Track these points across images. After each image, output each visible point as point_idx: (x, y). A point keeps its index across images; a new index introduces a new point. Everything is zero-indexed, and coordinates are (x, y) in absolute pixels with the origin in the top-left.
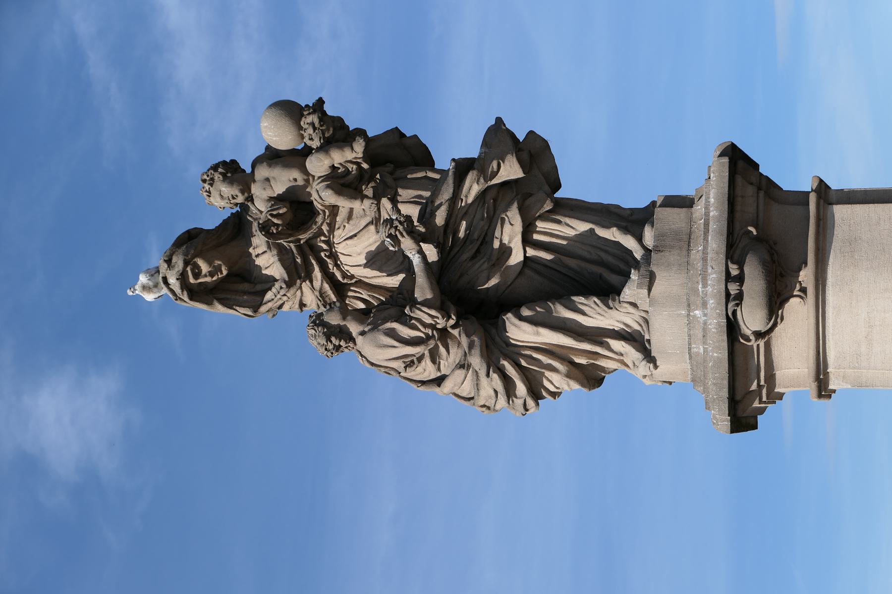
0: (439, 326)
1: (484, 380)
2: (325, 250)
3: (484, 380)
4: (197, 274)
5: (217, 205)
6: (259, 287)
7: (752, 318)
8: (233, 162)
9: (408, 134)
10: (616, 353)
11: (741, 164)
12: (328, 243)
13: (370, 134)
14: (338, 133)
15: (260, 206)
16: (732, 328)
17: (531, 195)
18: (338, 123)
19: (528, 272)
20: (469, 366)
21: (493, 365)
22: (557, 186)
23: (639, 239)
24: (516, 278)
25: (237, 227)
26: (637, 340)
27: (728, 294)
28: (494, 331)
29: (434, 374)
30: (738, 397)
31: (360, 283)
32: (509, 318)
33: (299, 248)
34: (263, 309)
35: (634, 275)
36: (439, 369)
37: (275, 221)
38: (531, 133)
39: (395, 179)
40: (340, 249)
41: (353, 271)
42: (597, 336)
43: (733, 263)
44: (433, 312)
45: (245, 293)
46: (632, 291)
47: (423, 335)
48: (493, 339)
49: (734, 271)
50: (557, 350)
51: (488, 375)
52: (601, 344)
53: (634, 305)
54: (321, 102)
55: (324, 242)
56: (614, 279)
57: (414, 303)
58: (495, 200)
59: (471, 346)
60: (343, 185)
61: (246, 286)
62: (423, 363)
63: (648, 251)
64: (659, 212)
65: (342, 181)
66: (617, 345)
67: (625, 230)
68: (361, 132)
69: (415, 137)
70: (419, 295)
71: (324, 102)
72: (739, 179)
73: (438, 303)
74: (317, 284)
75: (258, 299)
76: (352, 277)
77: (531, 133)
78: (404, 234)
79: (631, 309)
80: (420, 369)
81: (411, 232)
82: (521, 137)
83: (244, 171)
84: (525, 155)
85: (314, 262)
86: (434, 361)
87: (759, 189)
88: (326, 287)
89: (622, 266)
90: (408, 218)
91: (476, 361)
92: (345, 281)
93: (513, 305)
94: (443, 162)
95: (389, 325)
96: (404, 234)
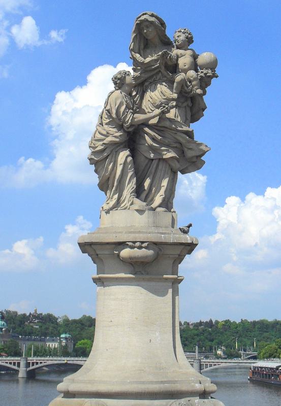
1: (101, 143)
2: (156, 78)
3: (101, 143)
4: (147, 27)
5: (174, 33)
6: (142, 52)
7: (125, 253)
8: (193, 41)
10: (112, 196)
11: (189, 248)
12: (160, 79)
13: (204, 97)
14: (204, 82)
15: (175, 52)
16: (122, 245)
17: (179, 162)
18: (208, 84)
19: (147, 161)
20: (107, 136)
21: (107, 146)
22: (183, 172)
23: (160, 206)
24: (145, 156)
25: (167, 43)
26: (117, 205)
27: (134, 242)
28: (122, 146)
29: (104, 122)
30: (92, 246)
32: (127, 152)
33: (158, 67)
34: (133, 53)
35: (145, 204)
38: (204, 162)
39: (185, 107)
42: (120, 190)
43: (148, 244)
44: (130, 121)
45: (139, 46)
46: (139, 204)
48: (119, 146)
49: (144, 245)
50: (113, 172)
51: (104, 144)
52: (116, 190)
53: (132, 204)
54: (217, 77)
55: (160, 78)
56: (143, 195)
57: (133, 113)
58: (176, 147)
59: (115, 137)
60: (182, 86)
61: (142, 47)
63: (154, 210)
64: (169, 214)
65: (184, 85)
66: (116, 196)
67: (164, 200)
68: (205, 93)
70: (136, 115)
72: (183, 247)
73: (133, 124)
74: (143, 75)
75: (137, 51)
77: (204, 162)
79: (130, 203)
81: (163, 113)
82: (202, 158)
83: (189, 46)
84: (195, 160)
85: (152, 74)
87: (179, 255)
88: (142, 79)
89: (150, 199)
90: (168, 112)
91: (110, 139)
93: (133, 154)
94: (193, 127)
95: (125, 103)
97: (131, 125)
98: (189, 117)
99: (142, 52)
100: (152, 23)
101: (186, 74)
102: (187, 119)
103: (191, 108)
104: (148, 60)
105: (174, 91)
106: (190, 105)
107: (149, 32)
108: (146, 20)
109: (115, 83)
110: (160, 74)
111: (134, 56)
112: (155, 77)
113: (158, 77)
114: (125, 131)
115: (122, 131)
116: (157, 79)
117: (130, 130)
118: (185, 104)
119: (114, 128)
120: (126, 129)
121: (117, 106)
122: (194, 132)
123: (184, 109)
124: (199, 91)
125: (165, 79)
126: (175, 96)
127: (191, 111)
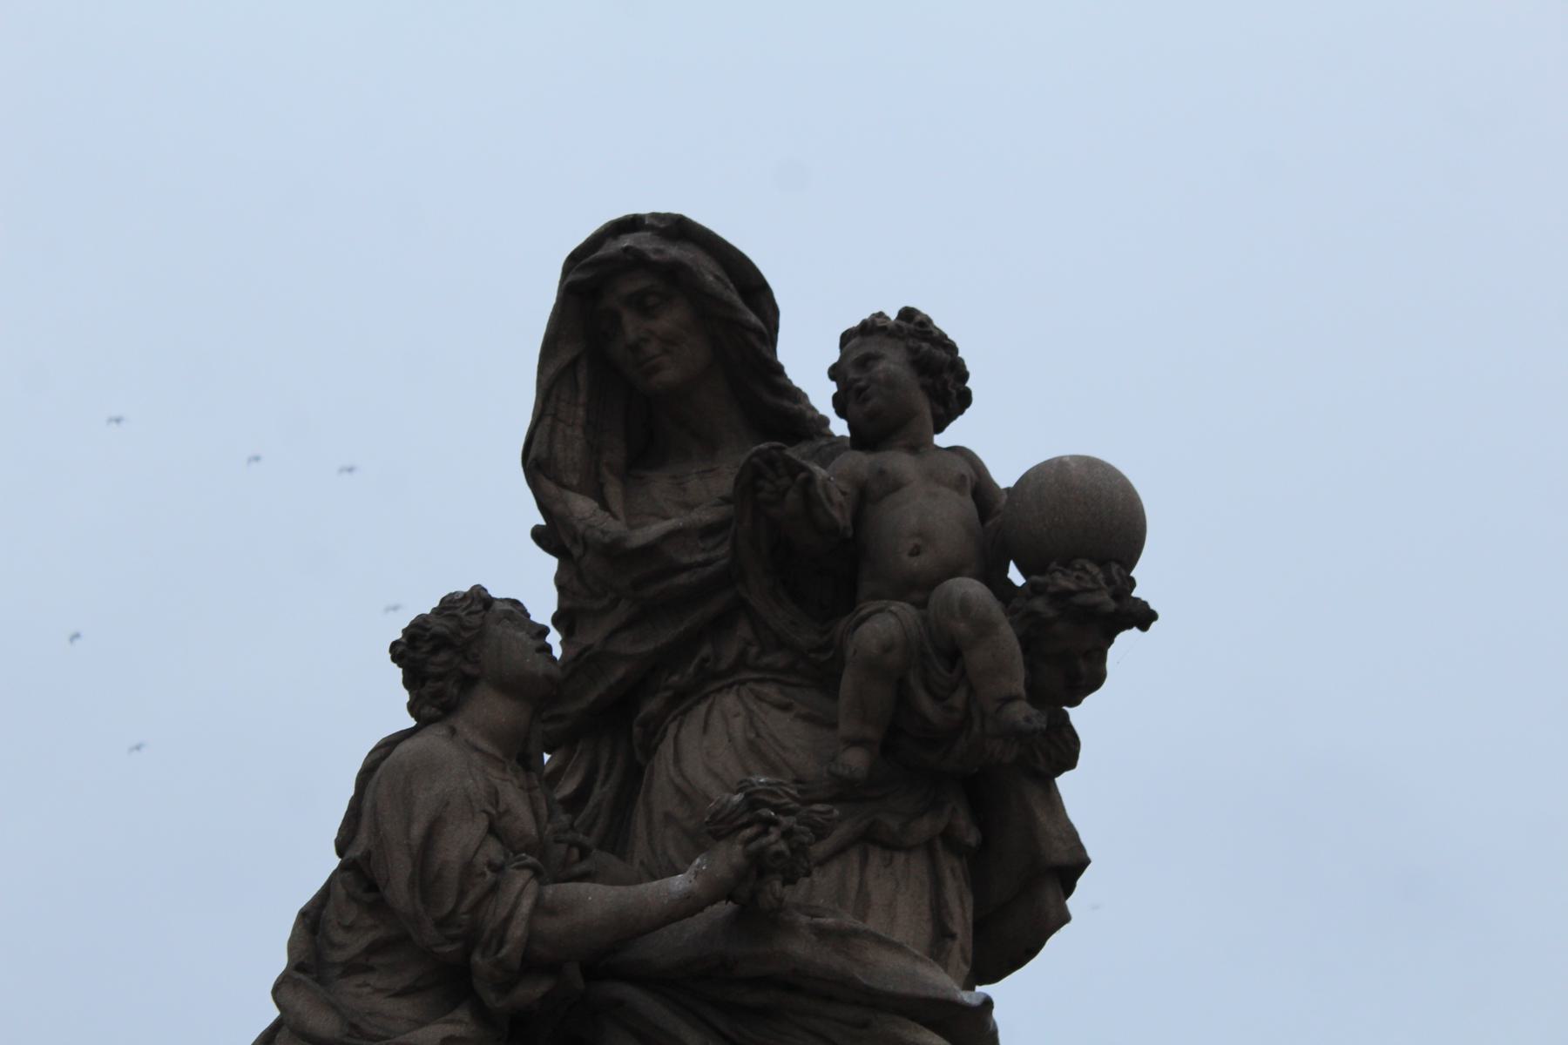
0: (477, 958)
4: (640, 304)
6: (614, 491)
8: (965, 399)
9: (1072, 903)
12: (741, 663)
13: (1066, 783)
31: (634, 777)
36: (351, 968)
37: (792, 496)
40: (729, 701)
41: (666, 748)
44: (517, 931)
47: (449, 905)
62: (369, 922)
69: (1065, 918)
71: (1144, 627)
76: (650, 751)
78: (753, 846)
80: (352, 914)
83: (939, 429)
86: (373, 949)
88: (620, 672)
92: (636, 730)
96: (753, 846)
97: (531, 965)
98: (961, 918)
99: (614, 491)
100: (674, 273)
101: (922, 605)
102: (941, 934)
103: (978, 866)
104: (656, 529)
105: (846, 728)
106: (973, 838)
107: (665, 344)
108: (635, 261)
109: (412, 681)
110: (744, 630)
111: (558, 508)
112: (706, 650)
113: (730, 653)
114: (482, 1014)
115: (463, 1014)
116: (723, 666)
117: (532, 991)
118: (925, 827)
119: (399, 994)
120: (491, 998)
121: (417, 830)
122: (997, 1014)
123: (919, 865)
124: (1021, 712)
125: (779, 659)
126: (855, 761)
127: (978, 883)
